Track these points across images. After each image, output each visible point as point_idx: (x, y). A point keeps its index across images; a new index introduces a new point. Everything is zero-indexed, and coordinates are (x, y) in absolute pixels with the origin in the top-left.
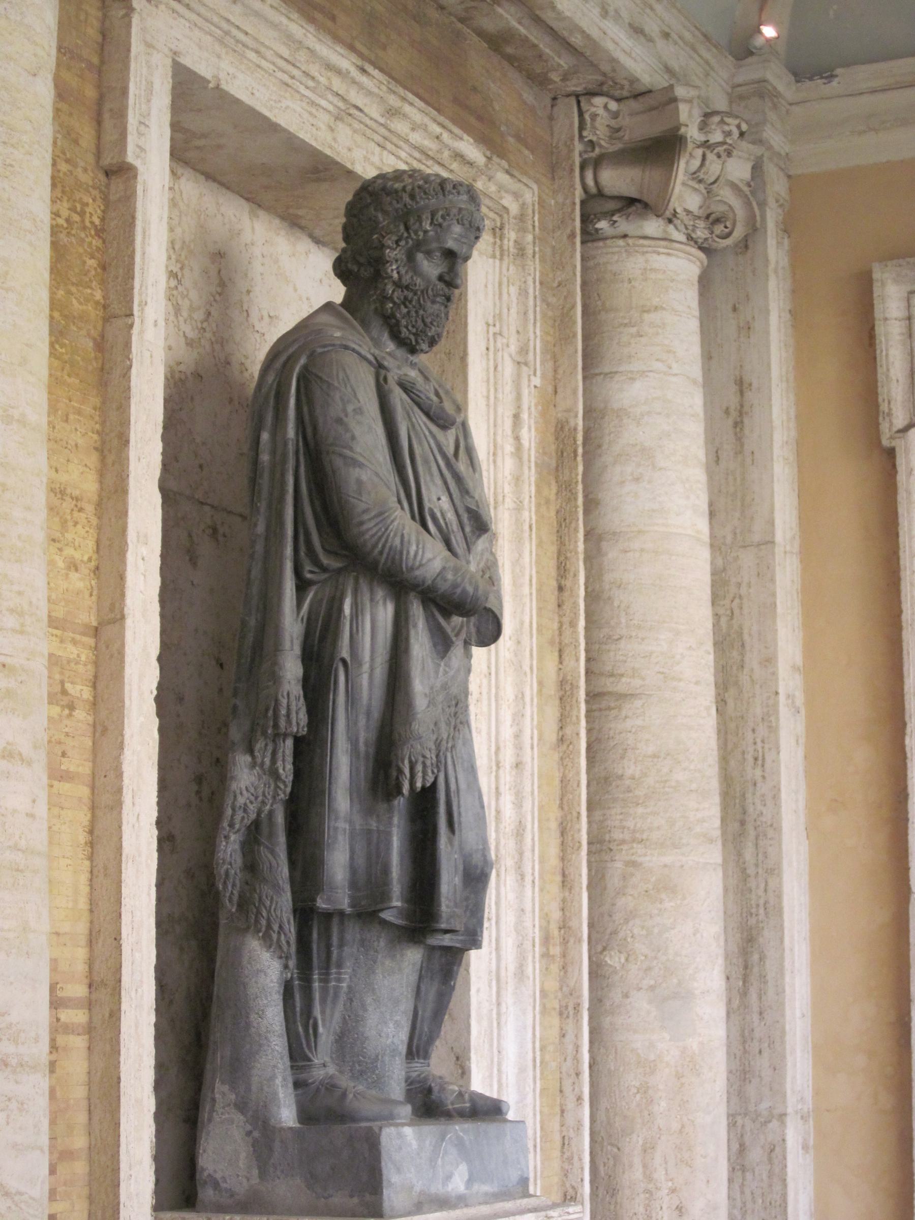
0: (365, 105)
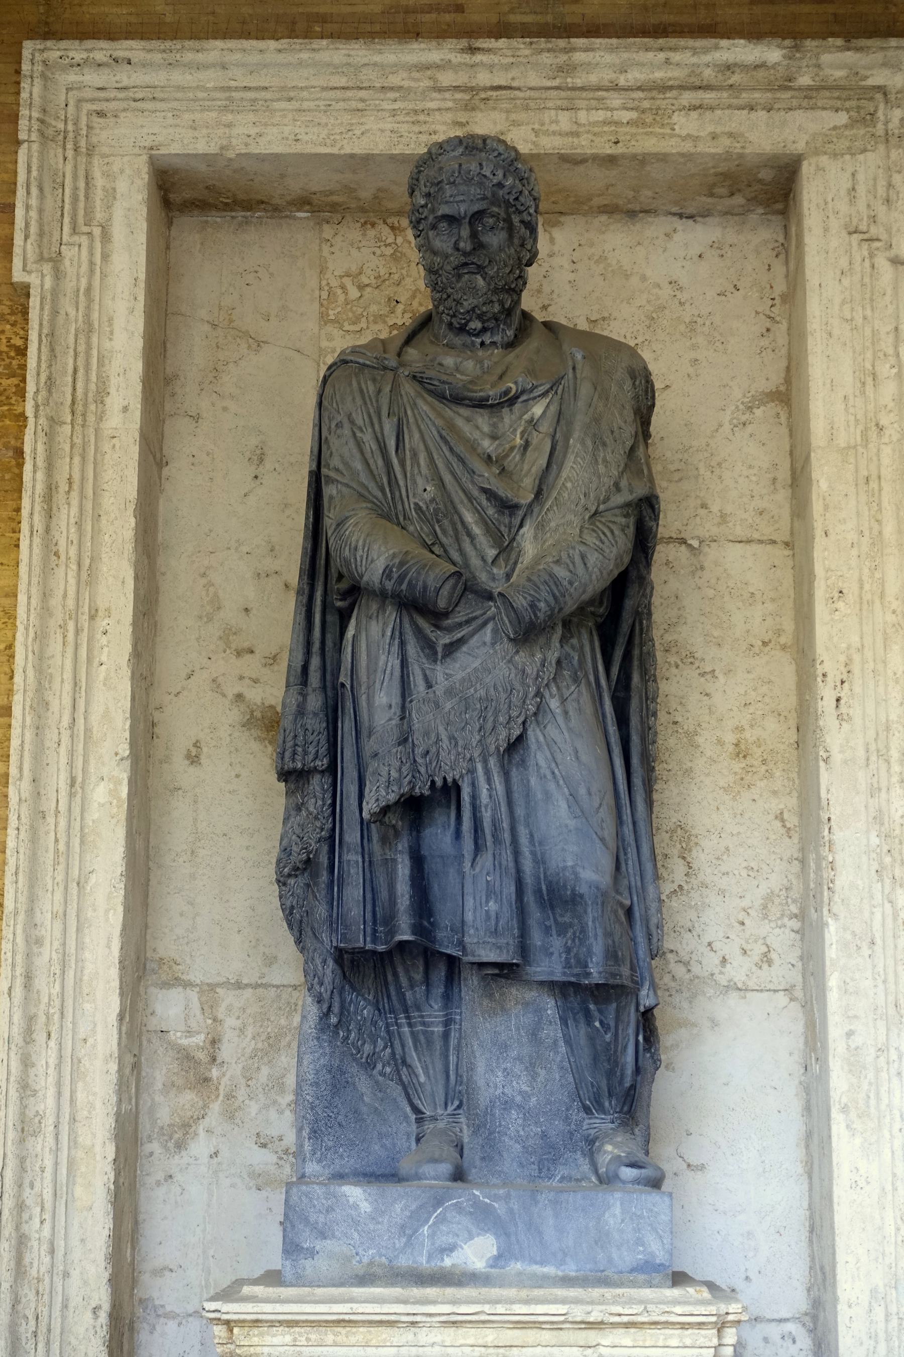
0: (513, 79)
